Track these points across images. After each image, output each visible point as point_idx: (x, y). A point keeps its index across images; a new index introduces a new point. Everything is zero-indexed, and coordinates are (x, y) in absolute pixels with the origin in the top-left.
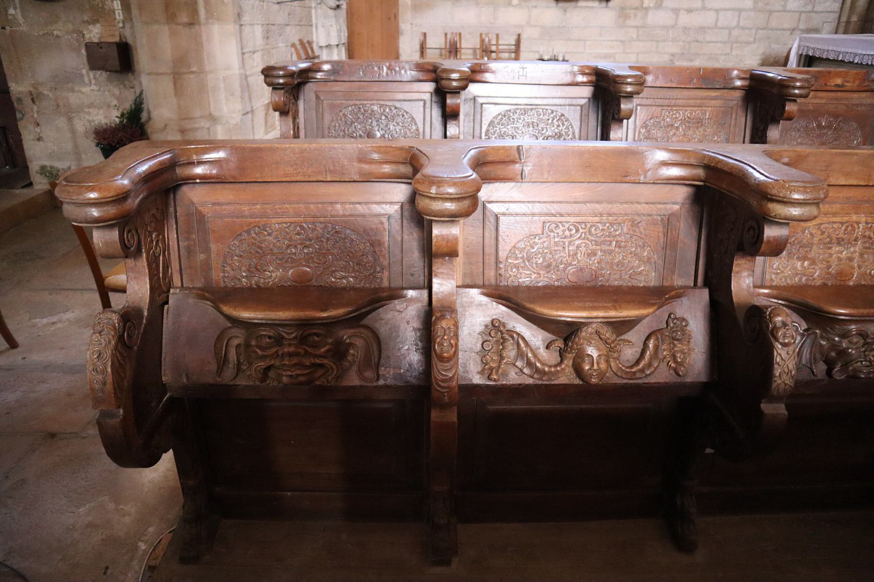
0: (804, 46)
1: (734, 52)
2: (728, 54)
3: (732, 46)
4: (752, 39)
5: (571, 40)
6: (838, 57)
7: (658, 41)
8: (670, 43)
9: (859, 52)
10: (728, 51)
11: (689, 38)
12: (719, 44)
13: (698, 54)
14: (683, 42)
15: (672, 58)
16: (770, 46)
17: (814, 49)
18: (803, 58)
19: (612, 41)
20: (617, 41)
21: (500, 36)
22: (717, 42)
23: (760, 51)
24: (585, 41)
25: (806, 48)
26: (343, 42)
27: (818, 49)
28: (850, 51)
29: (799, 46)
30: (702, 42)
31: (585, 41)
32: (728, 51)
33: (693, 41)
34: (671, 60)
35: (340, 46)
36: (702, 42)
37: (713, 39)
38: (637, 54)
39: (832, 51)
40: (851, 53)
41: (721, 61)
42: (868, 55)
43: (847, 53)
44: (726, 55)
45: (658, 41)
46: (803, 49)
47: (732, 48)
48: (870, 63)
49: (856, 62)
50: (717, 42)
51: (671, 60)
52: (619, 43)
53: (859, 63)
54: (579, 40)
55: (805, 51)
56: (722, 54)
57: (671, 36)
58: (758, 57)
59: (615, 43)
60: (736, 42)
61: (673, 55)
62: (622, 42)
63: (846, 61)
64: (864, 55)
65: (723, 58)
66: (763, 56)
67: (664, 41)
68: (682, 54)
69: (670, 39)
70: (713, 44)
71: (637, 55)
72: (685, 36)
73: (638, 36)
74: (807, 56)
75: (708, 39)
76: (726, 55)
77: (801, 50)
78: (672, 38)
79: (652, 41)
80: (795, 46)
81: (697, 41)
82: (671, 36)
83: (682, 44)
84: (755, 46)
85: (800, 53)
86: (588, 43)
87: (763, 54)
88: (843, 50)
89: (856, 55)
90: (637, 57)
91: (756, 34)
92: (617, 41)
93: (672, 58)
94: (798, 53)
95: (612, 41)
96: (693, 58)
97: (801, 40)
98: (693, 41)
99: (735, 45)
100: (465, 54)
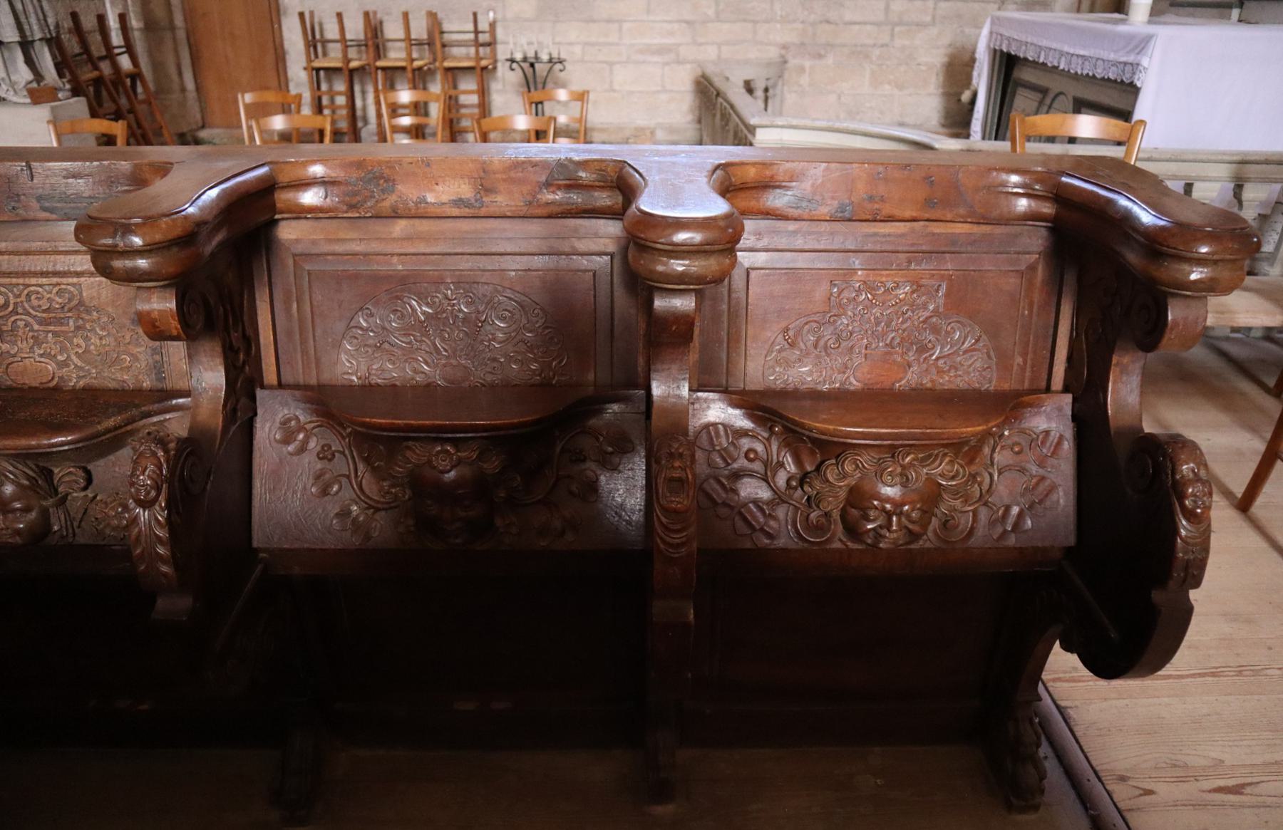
0: (997, 34)
1: (898, 42)
2: (887, 45)
3: (893, 30)
4: (928, 19)
5: (594, 21)
6: (1039, 57)
7: (755, 22)
8: (778, 26)
9: (1066, 49)
10: (885, 38)
11: (813, 17)
12: (869, 27)
13: (832, 46)
14: (803, 22)
15: (783, 52)
16: (962, 32)
17: (1008, 39)
18: (998, 54)
19: (670, 22)
20: (679, 21)
21: (410, 16)
22: (865, 23)
23: (946, 40)
24: (620, 22)
25: (999, 37)
26: (38, 35)
27: (1014, 39)
28: (1054, 45)
29: (991, 33)
30: (837, 24)
31: (620, 22)
32: (885, 38)
33: (821, 22)
34: (783, 56)
35: (37, 45)
36: (837, 24)
37: (858, 18)
38: (719, 45)
39: (1032, 44)
40: (1055, 50)
41: (874, 59)
42: (1078, 56)
43: (1050, 49)
44: (882, 46)
45: (755, 22)
46: (996, 40)
47: (892, 35)
48: (1079, 72)
49: (1061, 67)
50: (865, 23)
51: (783, 56)
52: (684, 25)
53: (1066, 69)
54: (609, 21)
55: (998, 43)
56: (875, 45)
57: (779, 13)
58: (942, 51)
59: (676, 26)
60: (900, 23)
61: (785, 47)
62: (687, 22)
63: (1049, 65)
64: (1072, 55)
65: (877, 52)
66: (950, 50)
67: (767, 21)
68: (803, 44)
69: (778, 18)
70: (857, 27)
71: (719, 48)
72: (806, 13)
73: (717, 13)
74: (1002, 51)
75: (848, 16)
76: (882, 46)
77: (993, 40)
78: (781, 16)
79: (745, 21)
80: (985, 31)
81: (828, 22)
82: (779, 13)
83: (800, 26)
84: (934, 31)
85: (992, 46)
86: (626, 26)
87: (950, 45)
88: (1045, 43)
89: (1062, 54)
90: (720, 51)
91: (935, 9)
92: (679, 21)
93: (783, 52)
94: (988, 46)
95: (670, 22)
96: (823, 52)
97: (993, 23)
98: (821, 22)
99: (897, 29)
100: (400, 49)
